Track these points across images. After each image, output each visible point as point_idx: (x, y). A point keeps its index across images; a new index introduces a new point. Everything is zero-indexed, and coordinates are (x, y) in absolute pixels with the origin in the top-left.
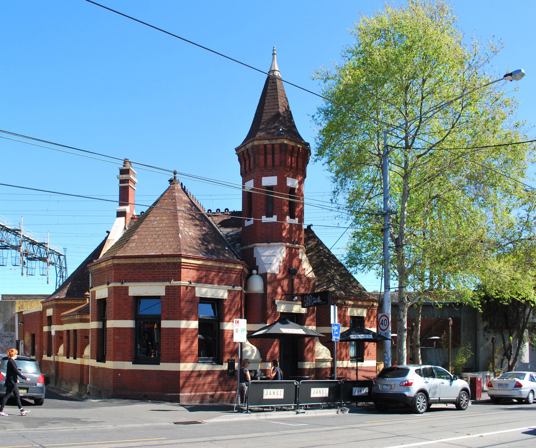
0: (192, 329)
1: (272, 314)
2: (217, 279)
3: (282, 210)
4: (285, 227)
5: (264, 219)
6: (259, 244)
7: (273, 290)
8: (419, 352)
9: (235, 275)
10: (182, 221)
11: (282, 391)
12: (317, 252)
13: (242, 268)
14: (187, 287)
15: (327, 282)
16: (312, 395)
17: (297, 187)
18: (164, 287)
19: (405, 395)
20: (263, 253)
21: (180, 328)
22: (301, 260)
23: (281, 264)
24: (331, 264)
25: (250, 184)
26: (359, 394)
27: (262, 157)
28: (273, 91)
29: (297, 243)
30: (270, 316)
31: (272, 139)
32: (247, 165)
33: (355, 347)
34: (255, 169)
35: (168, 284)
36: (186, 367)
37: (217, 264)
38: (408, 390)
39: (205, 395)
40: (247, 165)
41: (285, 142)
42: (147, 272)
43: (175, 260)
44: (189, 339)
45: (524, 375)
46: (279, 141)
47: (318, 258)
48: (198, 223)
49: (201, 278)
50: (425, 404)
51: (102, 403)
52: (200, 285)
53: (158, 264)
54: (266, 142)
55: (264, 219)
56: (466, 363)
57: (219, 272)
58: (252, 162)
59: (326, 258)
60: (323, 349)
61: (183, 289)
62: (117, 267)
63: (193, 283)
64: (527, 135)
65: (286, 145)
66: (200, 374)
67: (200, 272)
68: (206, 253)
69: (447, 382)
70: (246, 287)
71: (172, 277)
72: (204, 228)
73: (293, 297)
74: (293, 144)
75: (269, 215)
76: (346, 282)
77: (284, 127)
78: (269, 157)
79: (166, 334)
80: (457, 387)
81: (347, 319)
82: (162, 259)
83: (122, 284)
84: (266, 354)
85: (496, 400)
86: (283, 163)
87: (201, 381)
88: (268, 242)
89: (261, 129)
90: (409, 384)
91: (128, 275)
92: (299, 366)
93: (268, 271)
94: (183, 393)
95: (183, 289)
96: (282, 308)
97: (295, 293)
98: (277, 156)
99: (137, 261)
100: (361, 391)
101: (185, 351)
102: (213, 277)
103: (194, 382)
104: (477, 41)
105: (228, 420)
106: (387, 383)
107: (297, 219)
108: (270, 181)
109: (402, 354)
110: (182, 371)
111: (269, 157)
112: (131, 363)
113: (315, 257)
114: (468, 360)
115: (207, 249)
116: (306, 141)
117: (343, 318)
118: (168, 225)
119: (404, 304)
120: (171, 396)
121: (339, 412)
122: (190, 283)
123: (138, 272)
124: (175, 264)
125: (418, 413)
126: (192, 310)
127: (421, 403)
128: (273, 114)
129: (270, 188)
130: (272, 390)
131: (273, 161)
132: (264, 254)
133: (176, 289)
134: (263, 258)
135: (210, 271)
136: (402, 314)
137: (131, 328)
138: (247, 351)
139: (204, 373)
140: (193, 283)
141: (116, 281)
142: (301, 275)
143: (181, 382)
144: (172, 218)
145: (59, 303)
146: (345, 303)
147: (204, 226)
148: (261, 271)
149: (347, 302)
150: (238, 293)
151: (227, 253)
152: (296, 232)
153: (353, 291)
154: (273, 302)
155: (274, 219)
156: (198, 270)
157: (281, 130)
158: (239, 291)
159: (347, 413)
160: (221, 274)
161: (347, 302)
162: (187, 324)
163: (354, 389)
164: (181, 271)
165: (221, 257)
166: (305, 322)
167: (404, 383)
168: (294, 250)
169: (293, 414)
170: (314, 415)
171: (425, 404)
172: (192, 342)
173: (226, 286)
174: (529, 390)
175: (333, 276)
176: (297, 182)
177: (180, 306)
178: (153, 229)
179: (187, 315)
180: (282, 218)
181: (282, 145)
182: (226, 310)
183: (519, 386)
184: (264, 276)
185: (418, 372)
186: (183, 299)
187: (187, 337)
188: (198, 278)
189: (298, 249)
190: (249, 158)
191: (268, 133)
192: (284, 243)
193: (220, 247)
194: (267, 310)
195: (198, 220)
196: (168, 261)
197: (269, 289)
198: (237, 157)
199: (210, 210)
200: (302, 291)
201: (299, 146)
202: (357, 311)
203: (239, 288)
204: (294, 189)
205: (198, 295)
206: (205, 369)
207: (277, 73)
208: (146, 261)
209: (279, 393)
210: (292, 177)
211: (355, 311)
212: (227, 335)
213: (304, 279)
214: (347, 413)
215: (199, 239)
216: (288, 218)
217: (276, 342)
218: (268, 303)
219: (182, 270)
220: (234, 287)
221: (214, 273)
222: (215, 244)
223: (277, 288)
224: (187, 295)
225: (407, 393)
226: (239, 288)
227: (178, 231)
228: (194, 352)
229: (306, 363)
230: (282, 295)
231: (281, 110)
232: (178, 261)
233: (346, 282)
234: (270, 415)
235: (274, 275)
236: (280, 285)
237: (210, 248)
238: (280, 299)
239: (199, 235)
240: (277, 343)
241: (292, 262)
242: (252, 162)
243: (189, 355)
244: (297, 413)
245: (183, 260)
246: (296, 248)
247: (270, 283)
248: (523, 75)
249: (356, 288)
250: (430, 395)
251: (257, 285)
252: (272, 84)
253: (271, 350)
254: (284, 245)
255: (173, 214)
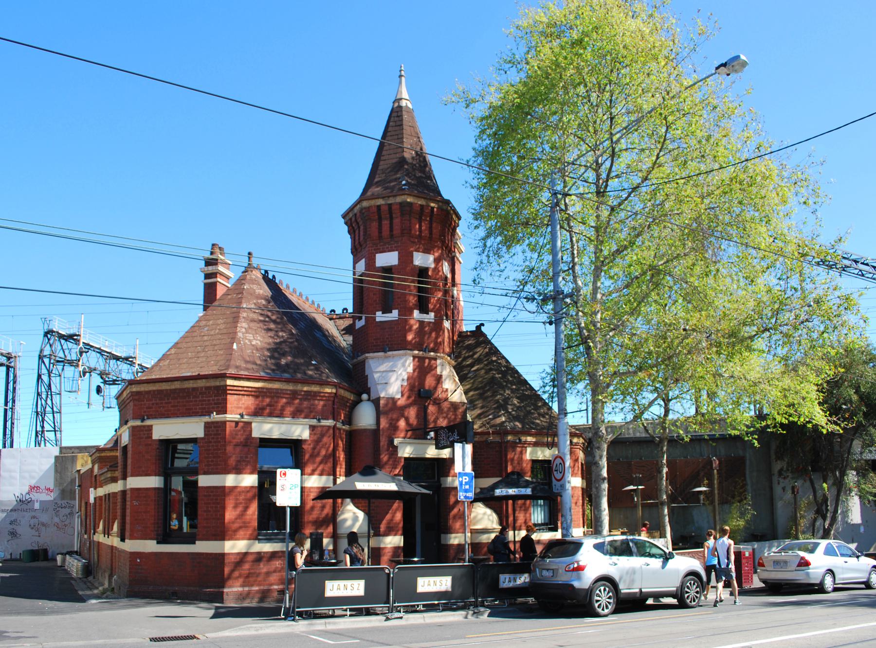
0: (246, 487)
1: (388, 460)
2: (289, 410)
3: (406, 301)
4: (411, 326)
5: (380, 317)
6: (371, 355)
7: (391, 424)
8: (666, 511)
9: (322, 403)
10: (245, 325)
11: (362, 583)
12: (486, 365)
13: (334, 391)
14: (237, 423)
15: (495, 408)
16: (420, 589)
17: (433, 266)
18: (203, 425)
19: (572, 586)
20: (378, 367)
21: (225, 487)
22: (441, 376)
23: (405, 384)
24: (508, 381)
25: (361, 266)
26: (511, 585)
27: (375, 224)
28: (397, 128)
29: (433, 350)
30: (386, 463)
31: (389, 197)
32: (357, 238)
33: (546, 508)
34: (366, 242)
35: (206, 419)
36: (234, 546)
37: (290, 387)
38: (579, 578)
39: (269, 591)
40: (357, 238)
41: (408, 200)
42: (178, 402)
43: (217, 383)
44: (241, 503)
45: (816, 545)
46: (399, 199)
47: (486, 373)
48: (272, 326)
49: (263, 409)
50: (611, 601)
51: (106, 605)
52: (260, 419)
53: (194, 389)
54: (380, 202)
55: (380, 317)
56: (745, 527)
57: (294, 398)
58: (362, 233)
59: (501, 372)
60: (485, 514)
61: (229, 428)
62: (136, 397)
63: (245, 417)
64: (784, 163)
65: (410, 204)
66: (260, 557)
67: (260, 399)
68: (273, 370)
69: (656, 563)
70: (349, 420)
71: (213, 408)
72: (281, 334)
73: (427, 433)
74: (421, 202)
75: (387, 310)
76: (528, 409)
77: (410, 177)
78: (386, 223)
79: (205, 496)
80: (678, 571)
81: (524, 465)
82: (199, 381)
83: (142, 421)
84: (380, 524)
85: (774, 588)
86: (406, 231)
87: (263, 568)
88: (385, 352)
89: (377, 182)
90: (580, 568)
91: (151, 408)
92: (443, 542)
93: (382, 395)
94: (230, 587)
95: (231, 427)
96: (406, 451)
97: (431, 426)
98: (397, 221)
99: (164, 386)
100: (515, 580)
101: (233, 523)
102: (283, 407)
103: (249, 569)
104: (674, 21)
105: (252, 632)
106: (547, 567)
107: (432, 315)
108: (388, 259)
109: (600, 517)
110: (229, 554)
111: (386, 223)
112: (155, 542)
113: (483, 372)
114: (747, 522)
115: (278, 365)
116: (446, 196)
117: (518, 463)
118: (222, 332)
119: (601, 437)
120: (211, 593)
121: (469, 617)
122: (242, 416)
123: (166, 403)
124: (217, 388)
125: (598, 615)
126: (247, 457)
127: (603, 598)
128: (394, 161)
129: (388, 270)
130: (342, 583)
131: (391, 229)
132: (378, 370)
133: (219, 427)
134: (376, 376)
135: (278, 397)
136: (597, 453)
137: (155, 489)
138: (345, 520)
139: (268, 555)
140: (245, 417)
141: (134, 418)
142: (440, 399)
143: (227, 570)
144: (231, 320)
145: (103, 455)
146: (520, 440)
147: (282, 331)
148: (373, 396)
149: (523, 439)
150: (328, 430)
151: (311, 370)
152: (430, 333)
153: (538, 421)
154: (391, 442)
155: (394, 315)
156: (257, 397)
157: (404, 182)
158: (329, 427)
159: (485, 616)
160: (297, 401)
161: (523, 439)
162: (236, 479)
163: (502, 577)
164: (226, 399)
165: (299, 376)
166: (449, 472)
167: (572, 567)
168: (427, 361)
169: (380, 621)
170: (421, 621)
171: (611, 601)
172: (246, 508)
173: (307, 420)
174: (823, 570)
175: (506, 400)
176: (431, 258)
177: (225, 453)
178: (199, 338)
179: (236, 465)
180: (406, 312)
181: (403, 205)
182: (307, 456)
183: (805, 563)
184: (376, 402)
185: (599, 547)
186: (230, 442)
187: (237, 499)
188: (256, 409)
189: (435, 359)
190: (359, 227)
191: (386, 188)
192: (409, 352)
193: (302, 361)
194: (380, 455)
195: (274, 322)
196: (208, 385)
197: (384, 423)
198: (346, 228)
199: (334, 311)
200: (442, 422)
201: (432, 205)
202: (543, 452)
203: (329, 423)
204: (427, 269)
205: (256, 434)
206: (271, 550)
207: (403, 103)
208: (177, 385)
209: (356, 586)
210: (424, 252)
211: (539, 453)
212: (308, 495)
213: (445, 405)
214: (485, 616)
215: (268, 350)
216: (416, 313)
217: (397, 505)
218: (382, 444)
219: (229, 397)
220: (319, 420)
221: (284, 400)
222: (294, 356)
223: (398, 420)
224: (236, 435)
225: (576, 584)
226: (329, 423)
227: (233, 339)
228: (249, 523)
229: (453, 535)
230: (407, 431)
231: (408, 155)
232: (222, 383)
233: (528, 409)
234: (334, 623)
235: (392, 401)
236: (403, 415)
237: (283, 362)
238: (404, 438)
239: (269, 344)
240: (399, 506)
241: (424, 380)
242: (362, 233)
243: (241, 527)
244: (388, 619)
245: (229, 382)
246: (431, 359)
247: (386, 413)
248: (744, 64)
249: (544, 417)
250: (621, 586)
251: (365, 417)
252: (396, 119)
253: (388, 517)
254: (410, 355)
255: (234, 315)
